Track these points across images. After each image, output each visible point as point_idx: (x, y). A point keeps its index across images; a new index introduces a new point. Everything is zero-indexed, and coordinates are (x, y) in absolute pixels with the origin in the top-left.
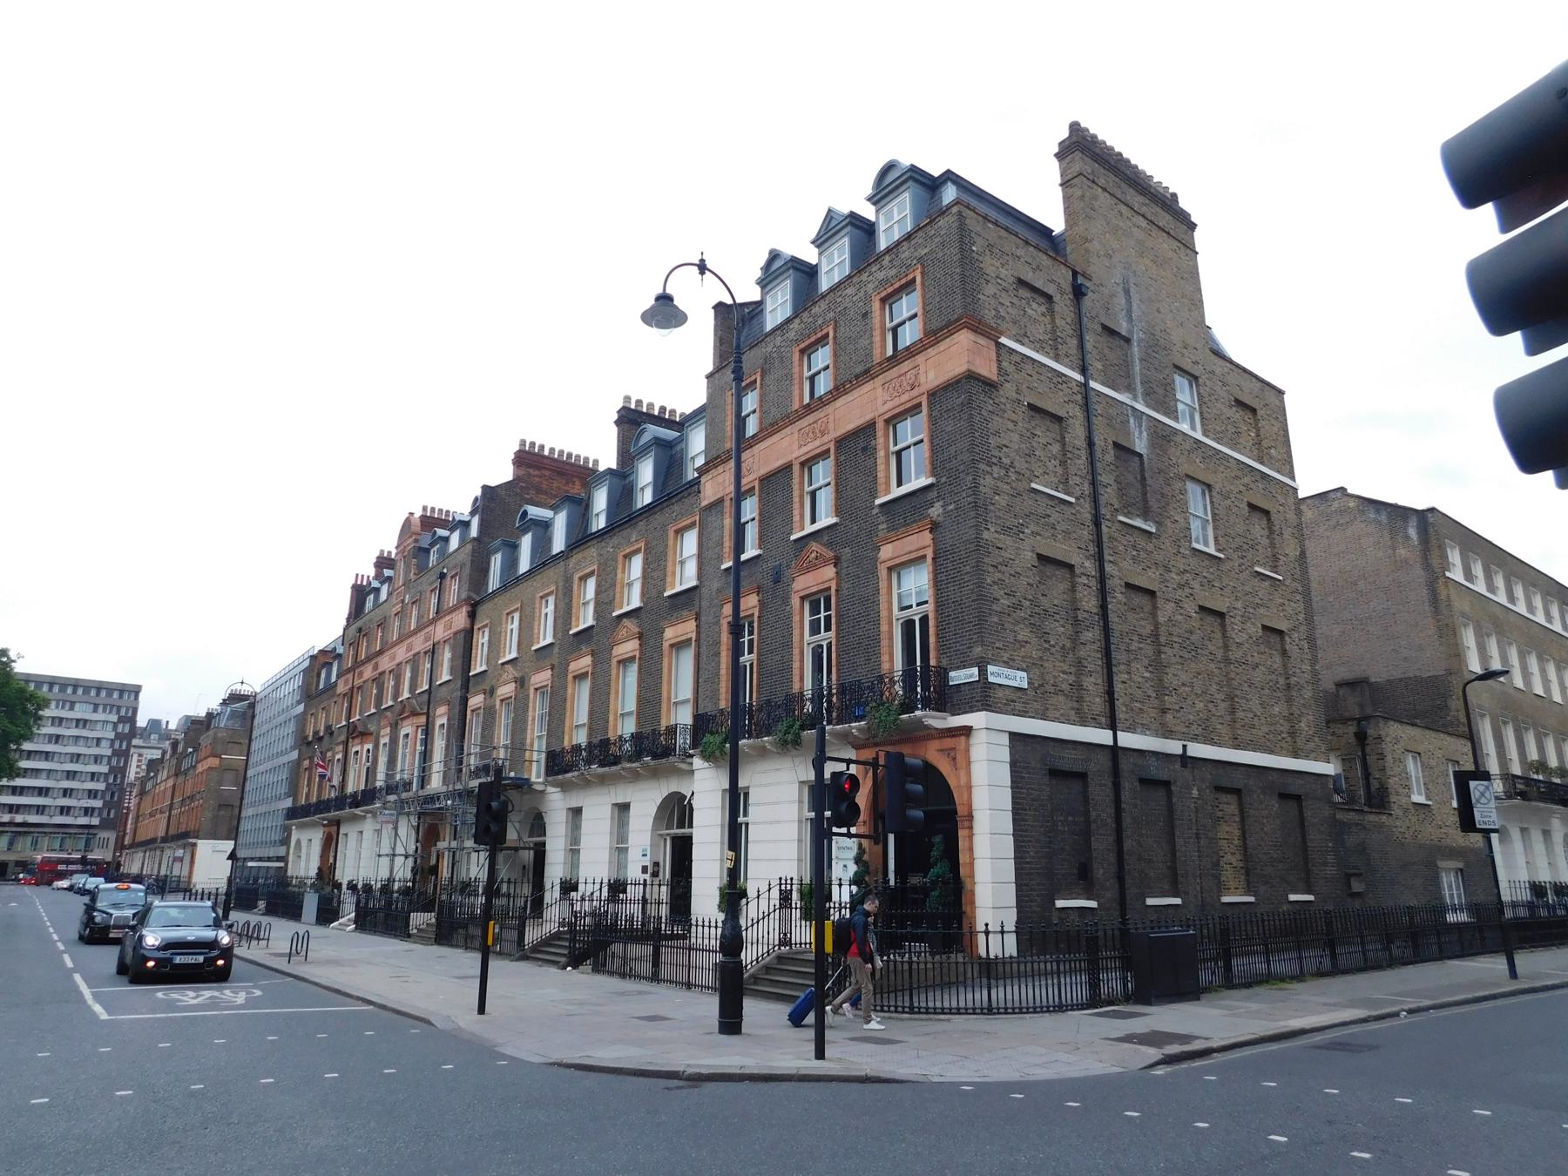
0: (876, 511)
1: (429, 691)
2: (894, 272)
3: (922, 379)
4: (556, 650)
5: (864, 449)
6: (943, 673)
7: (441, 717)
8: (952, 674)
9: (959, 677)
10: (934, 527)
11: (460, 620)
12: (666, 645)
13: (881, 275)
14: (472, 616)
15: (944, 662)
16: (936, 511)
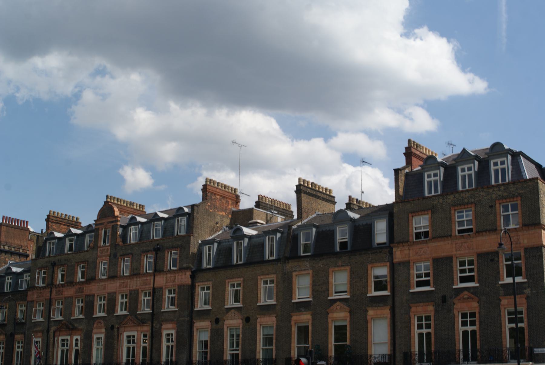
0: (497, 285)
1: (153, 314)
2: (505, 194)
3: (521, 241)
4: (278, 307)
5: (492, 260)
6: (531, 349)
7: (168, 330)
8: (535, 350)
9: (537, 351)
10: (527, 298)
11: (185, 278)
12: (369, 317)
13: (500, 193)
14: (193, 277)
15: (531, 345)
16: (528, 291)
